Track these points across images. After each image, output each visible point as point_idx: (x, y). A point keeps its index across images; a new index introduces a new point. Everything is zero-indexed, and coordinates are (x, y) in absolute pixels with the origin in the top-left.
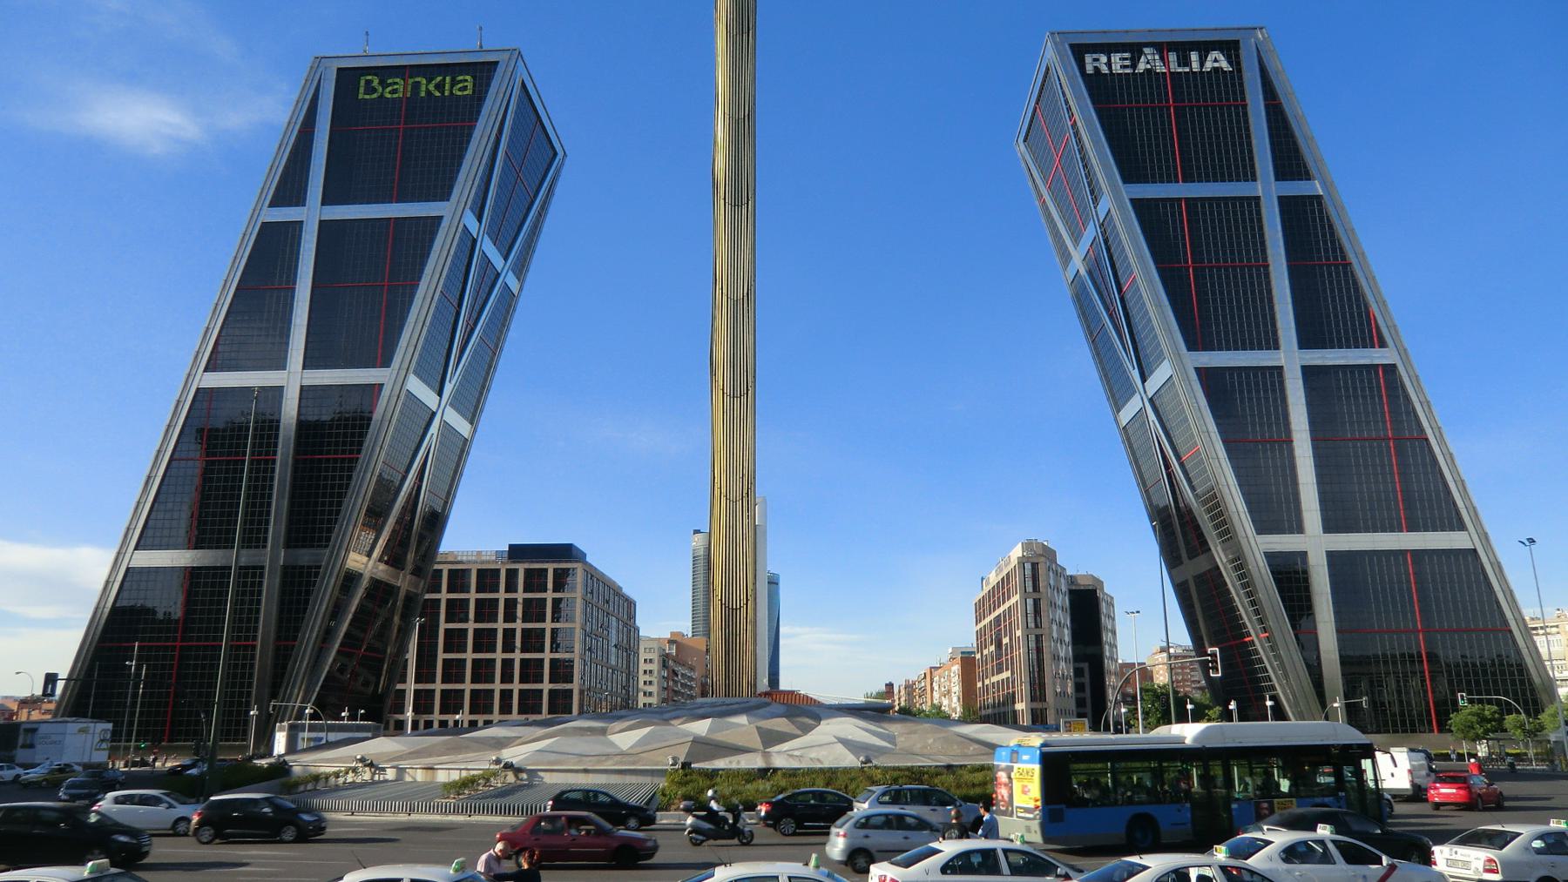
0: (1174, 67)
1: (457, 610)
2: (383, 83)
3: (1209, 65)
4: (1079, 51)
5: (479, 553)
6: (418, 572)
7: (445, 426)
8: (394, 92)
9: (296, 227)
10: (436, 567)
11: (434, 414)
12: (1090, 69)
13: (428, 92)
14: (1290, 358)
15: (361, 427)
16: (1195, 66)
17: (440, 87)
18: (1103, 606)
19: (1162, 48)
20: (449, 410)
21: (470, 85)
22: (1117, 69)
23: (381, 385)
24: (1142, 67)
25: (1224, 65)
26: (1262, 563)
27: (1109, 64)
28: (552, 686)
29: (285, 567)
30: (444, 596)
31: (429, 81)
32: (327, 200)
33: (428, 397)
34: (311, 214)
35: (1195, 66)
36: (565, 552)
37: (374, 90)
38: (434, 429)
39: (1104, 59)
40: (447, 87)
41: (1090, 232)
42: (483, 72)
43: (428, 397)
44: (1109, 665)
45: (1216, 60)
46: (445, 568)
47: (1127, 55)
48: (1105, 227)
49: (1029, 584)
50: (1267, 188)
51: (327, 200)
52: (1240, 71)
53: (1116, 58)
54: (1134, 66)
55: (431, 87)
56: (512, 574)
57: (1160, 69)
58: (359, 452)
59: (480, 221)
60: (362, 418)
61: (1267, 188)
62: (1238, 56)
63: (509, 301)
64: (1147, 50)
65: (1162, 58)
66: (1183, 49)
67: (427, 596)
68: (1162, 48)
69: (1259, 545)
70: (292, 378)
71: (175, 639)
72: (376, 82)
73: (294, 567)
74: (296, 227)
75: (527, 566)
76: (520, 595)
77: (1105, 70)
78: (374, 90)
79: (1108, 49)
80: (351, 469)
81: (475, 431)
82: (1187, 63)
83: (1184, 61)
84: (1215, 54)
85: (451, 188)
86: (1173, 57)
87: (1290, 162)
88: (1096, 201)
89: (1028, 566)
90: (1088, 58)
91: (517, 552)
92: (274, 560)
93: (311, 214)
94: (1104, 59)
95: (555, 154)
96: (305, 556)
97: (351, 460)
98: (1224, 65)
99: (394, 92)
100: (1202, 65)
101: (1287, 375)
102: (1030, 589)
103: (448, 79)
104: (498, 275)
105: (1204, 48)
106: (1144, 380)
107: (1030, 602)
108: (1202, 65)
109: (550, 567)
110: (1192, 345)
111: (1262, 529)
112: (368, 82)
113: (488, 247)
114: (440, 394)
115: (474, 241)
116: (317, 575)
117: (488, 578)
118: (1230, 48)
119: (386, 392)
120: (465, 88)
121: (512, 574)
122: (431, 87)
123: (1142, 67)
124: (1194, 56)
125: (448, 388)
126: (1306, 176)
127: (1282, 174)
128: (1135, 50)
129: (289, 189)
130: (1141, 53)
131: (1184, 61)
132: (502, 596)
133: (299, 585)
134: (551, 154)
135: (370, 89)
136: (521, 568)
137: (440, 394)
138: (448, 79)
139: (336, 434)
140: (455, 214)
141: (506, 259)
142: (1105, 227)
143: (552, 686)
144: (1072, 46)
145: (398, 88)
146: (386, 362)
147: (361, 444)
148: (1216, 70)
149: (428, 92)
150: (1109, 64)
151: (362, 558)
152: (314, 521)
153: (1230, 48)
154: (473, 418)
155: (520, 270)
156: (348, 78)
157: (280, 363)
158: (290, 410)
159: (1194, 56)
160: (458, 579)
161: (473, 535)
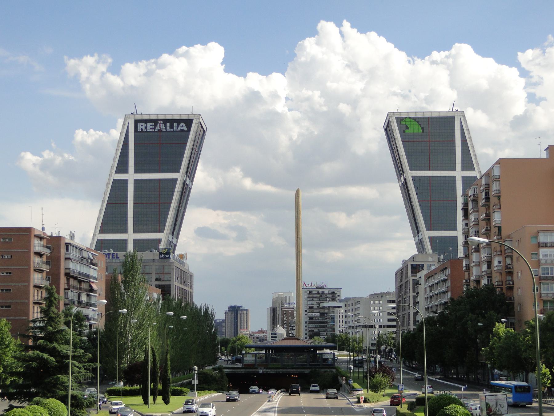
12: (139, 129)
22: (148, 129)
24: (157, 128)
27: (146, 128)
39: (144, 125)
45: (182, 127)
47: (151, 124)
53: (148, 125)
54: (155, 128)
57: (164, 130)
66: (172, 122)
68: (165, 121)
77: (144, 129)
83: (172, 127)
84: (182, 124)
86: (168, 125)
90: (139, 125)
98: (185, 128)
105: (179, 121)
118: (189, 122)
123: (157, 128)
124: (175, 125)
128: (155, 122)
131: (172, 127)
148: (182, 130)
150: (146, 128)
159: (175, 125)
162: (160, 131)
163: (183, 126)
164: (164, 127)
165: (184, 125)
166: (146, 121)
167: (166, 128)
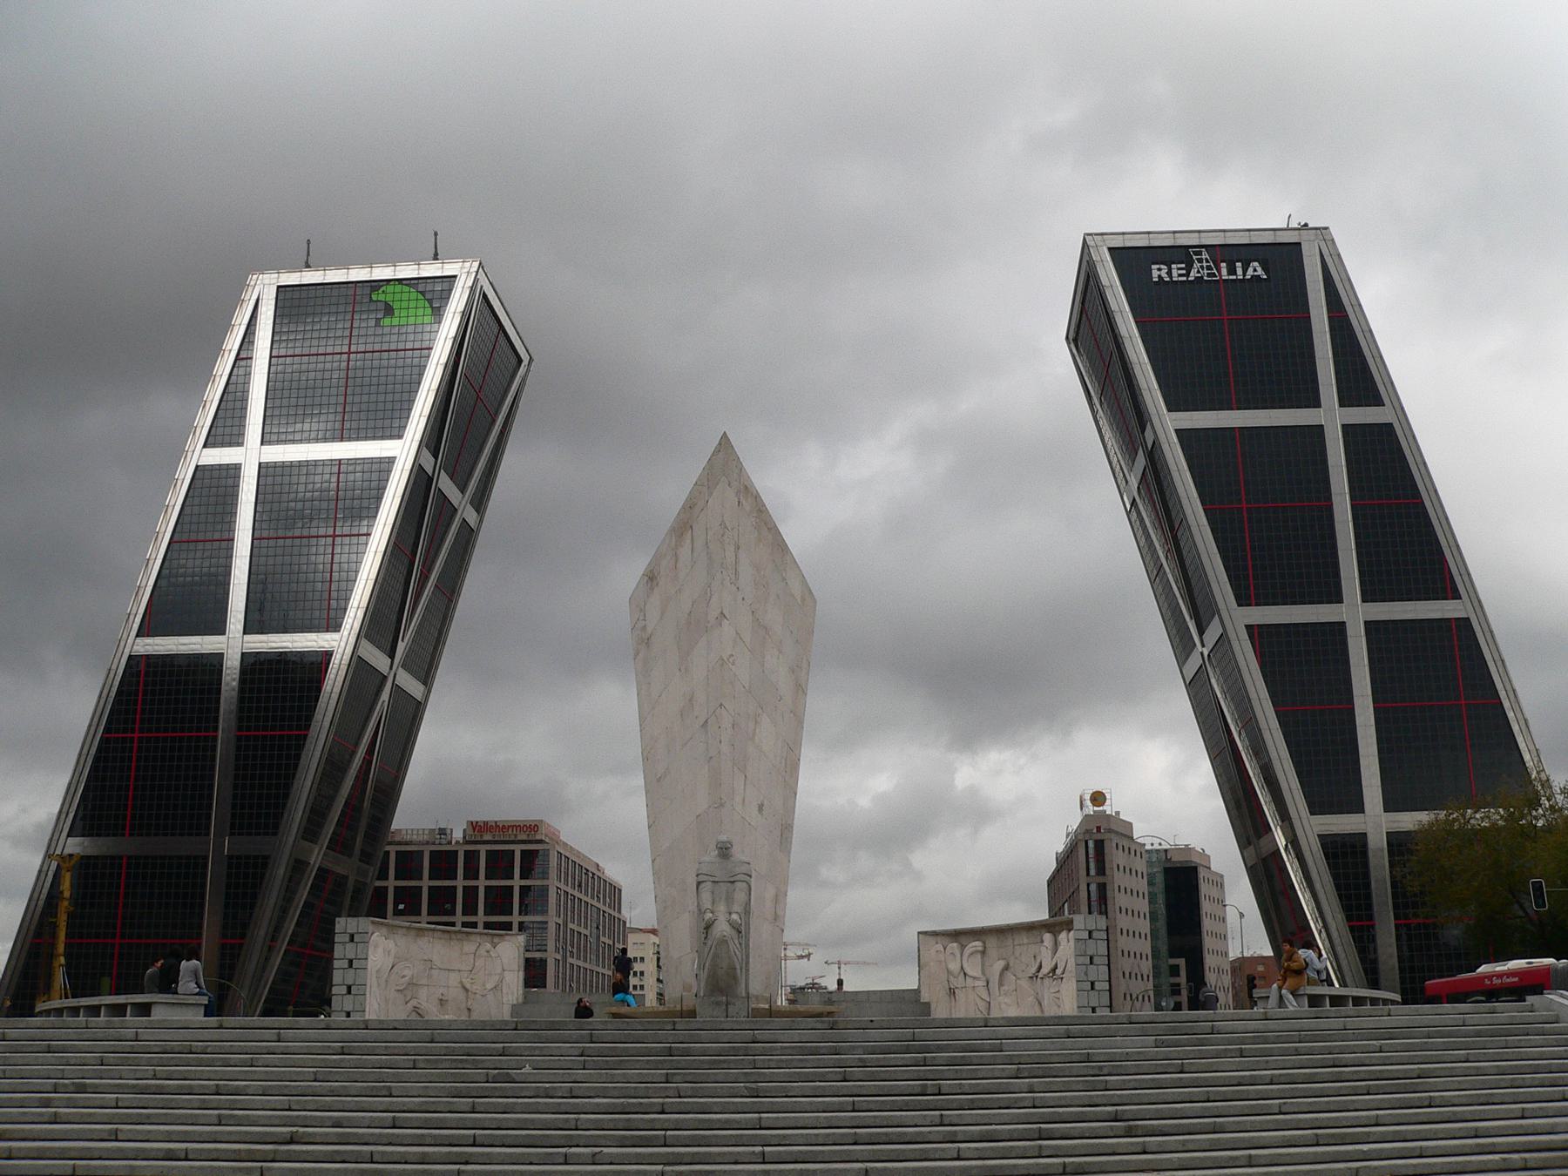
6: (366, 857)
7: (398, 690)
9: (234, 471)
10: (388, 848)
11: (385, 678)
14: (1354, 612)
18: (1204, 889)
26: (1316, 846)
29: (230, 857)
30: (391, 883)
33: (379, 661)
34: (250, 455)
38: (385, 696)
41: (1141, 460)
46: (392, 849)
49: (1092, 865)
50: (1331, 416)
56: (471, 857)
58: (308, 727)
59: (436, 458)
61: (1331, 416)
63: (468, 536)
67: (378, 883)
69: (1312, 827)
70: (233, 642)
73: (239, 857)
74: (234, 471)
75: (489, 847)
76: (482, 883)
81: (429, 691)
89: (1091, 844)
92: (219, 846)
95: (520, 361)
101: (1350, 632)
102: (1092, 872)
106: (1201, 632)
107: (1093, 887)
109: (517, 849)
111: (1317, 806)
113: (445, 484)
114: (392, 656)
116: (265, 865)
117: (444, 862)
119: (335, 660)
121: (471, 857)
125: (401, 647)
126: (1377, 401)
132: (460, 883)
134: (514, 361)
136: (483, 849)
137: (392, 656)
141: (463, 490)
142: (1155, 459)
146: (334, 625)
152: (260, 805)
154: (427, 678)
155: (480, 502)
157: (219, 628)
160: (408, 863)
167: (1219, 271)
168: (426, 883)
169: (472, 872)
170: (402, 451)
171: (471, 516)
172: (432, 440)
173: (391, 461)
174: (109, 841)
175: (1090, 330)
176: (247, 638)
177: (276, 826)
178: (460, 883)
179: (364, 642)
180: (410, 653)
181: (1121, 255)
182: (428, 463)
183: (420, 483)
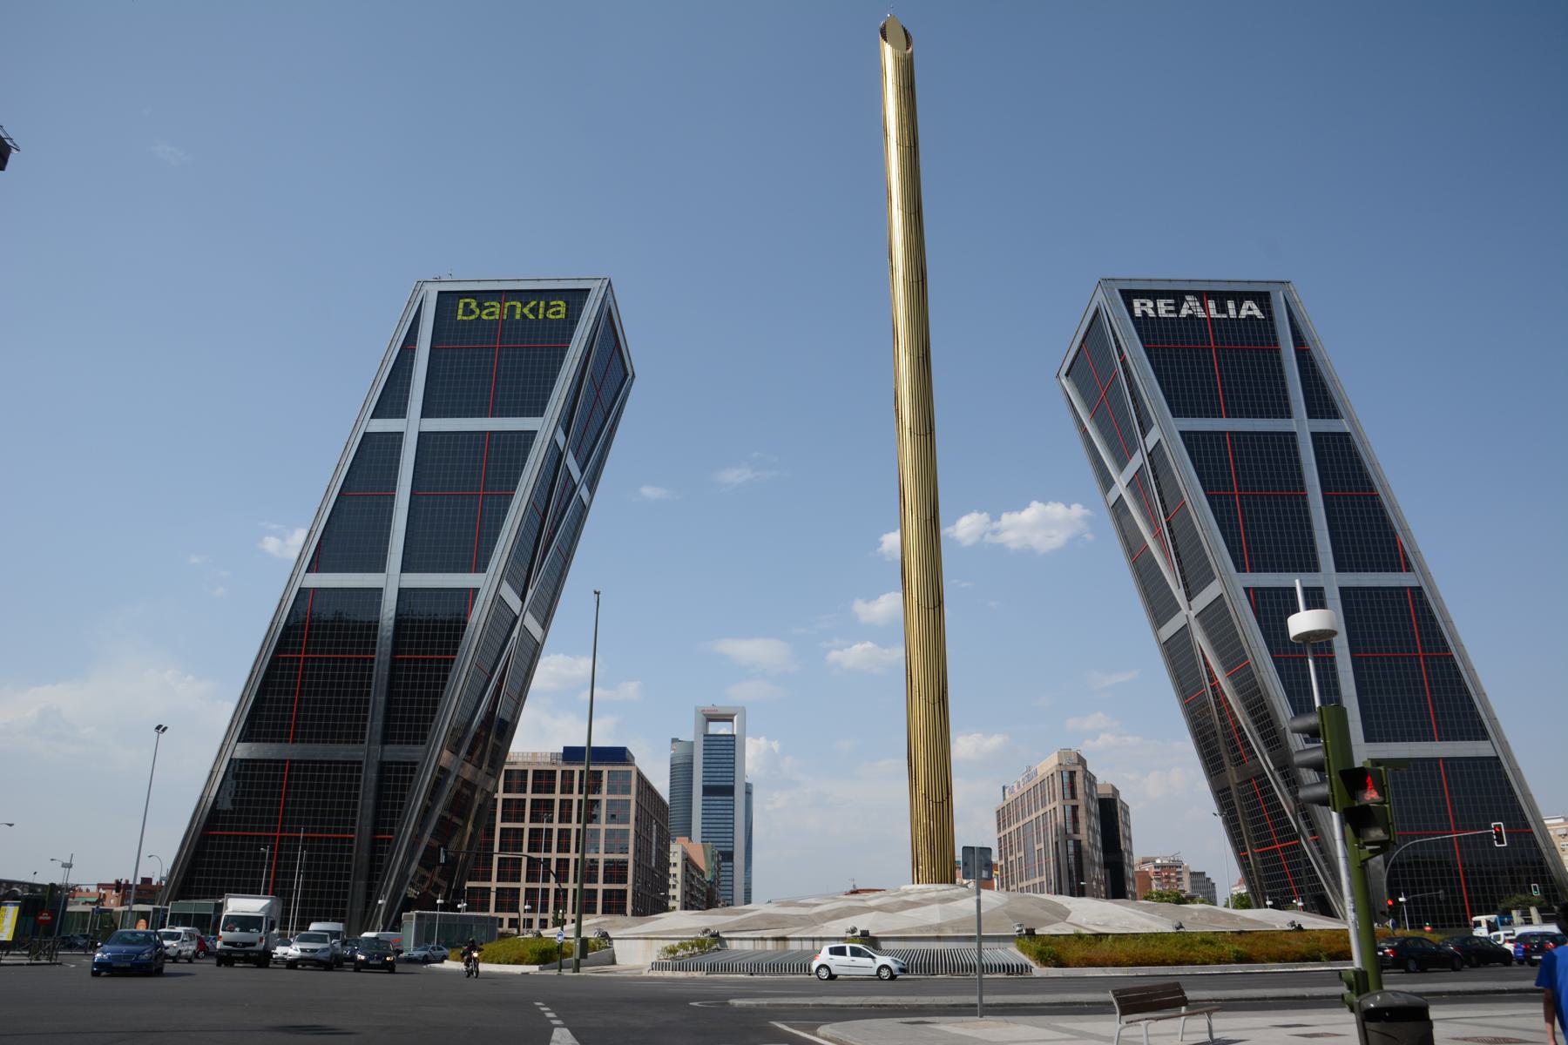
0: (1213, 313)
1: (513, 810)
2: (480, 306)
3: (1244, 313)
4: (1128, 296)
5: (534, 754)
7: (524, 629)
8: (492, 314)
11: (516, 618)
12: (1138, 313)
13: (524, 316)
15: (457, 629)
16: (1232, 313)
17: (534, 310)
19: (1202, 296)
20: (528, 615)
21: (563, 310)
22: (1162, 313)
23: (477, 590)
24: (1184, 312)
25: (1257, 313)
27: (1155, 309)
28: (607, 886)
31: (524, 305)
32: (426, 413)
33: (514, 601)
34: (412, 425)
35: (1232, 313)
36: (619, 755)
37: (472, 312)
38: (515, 634)
39: (1150, 304)
40: (541, 311)
42: (576, 298)
43: (514, 601)
44: (1129, 873)
48: (1156, 456)
49: (1067, 791)
50: (1302, 425)
51: (426, 413)
52: (1271, 319)
53: (1161, 303)
54: (1178, 311)
55: (526, 311)
56: (567, 776)
57: (1201, 315)
58: (455, 653)
60: (458, 621)
61: (1302, 425)
62: (1269, 306)
63: (583, 510)
64: (1188, 298)
65: (1202, 305)
66: (1221, 298)
68: (1202, 296)
71: (275, 830)
72: (473, 305)
77: (1151, 313)
78: (472, 312)
79: (1154, 295)
80: (447, 670)
82: (1225, 311)
83: (1222, 308)
84: (1247, 304)
85: (545, 404)
86: (1211, 304)
87: (1321, 401)
88: (1144, 434)
89: (1066, 775)
90: (1137, 303)
91: (571, 754)
93: (412, 425)
94: (1150, 304)
95: (626, 375)
96: (396, 752)
97: (446, 661)
98: (1257, 313)
99: (492, 314)
100: (1238, 313)
103: (542, 304)
104: (575, 487)
105: (1239, 297)
106: (1189, 597)
108: (1238, 313)
109: (605, 769)
110: (1240, 568)
112: (467, 305)
114: (523, 599)
115: (561, 455)
117: (544, 779)
118: (1263, 299)
119: (481, 597)
120: (558, 313)
121: (567, 776)
122: (526, 311)
123: (1184, 312)
124: (1231, 305)
125: (530, 592)
127: (1312, 414)
128: (1178, 297)
129: (391, 401)
130: (1183, 300)
131: (1222, 308)
132: (557, 796)
133: (395, 779)
135: (468, 310)
137: (523, 599)
138: (542, 304)
139: (432, 631)
140: (544, 427)
142: (1156, 456)
143: (607, 886)
144: (1121, 291)
145: (495, 310)
146: (481, 567)
147: (456, 645)
149: (524, 316)
150: (1155, 309)
151: (438, 754)
153: (1263, 299)
154: (545, 624)
156: (447, 300)
157: (379, 566)
158: (389, 609)
159: (1231, 305)
160: (516, 780)
161: (538, 737)
162: (1191, 317)
163: (1250, 309)
164: (1200, 309)
165: (1254, 306)
166: (1154, 295)
167: (1206, 310)
168: (529, 796)
169: (567, 789)
170: (544, 427)
171: (584, 492)
172: (566, 422)
173: (532, 434)
174: (274, 746)
175: (1091, 364)
176: (405, 575)
177: (424, 737)
178: (557, 796)
179: (505, 584)
180: (536, 598)
181: (1128, 296)
182: (561, 438)
183: (555, 458)
